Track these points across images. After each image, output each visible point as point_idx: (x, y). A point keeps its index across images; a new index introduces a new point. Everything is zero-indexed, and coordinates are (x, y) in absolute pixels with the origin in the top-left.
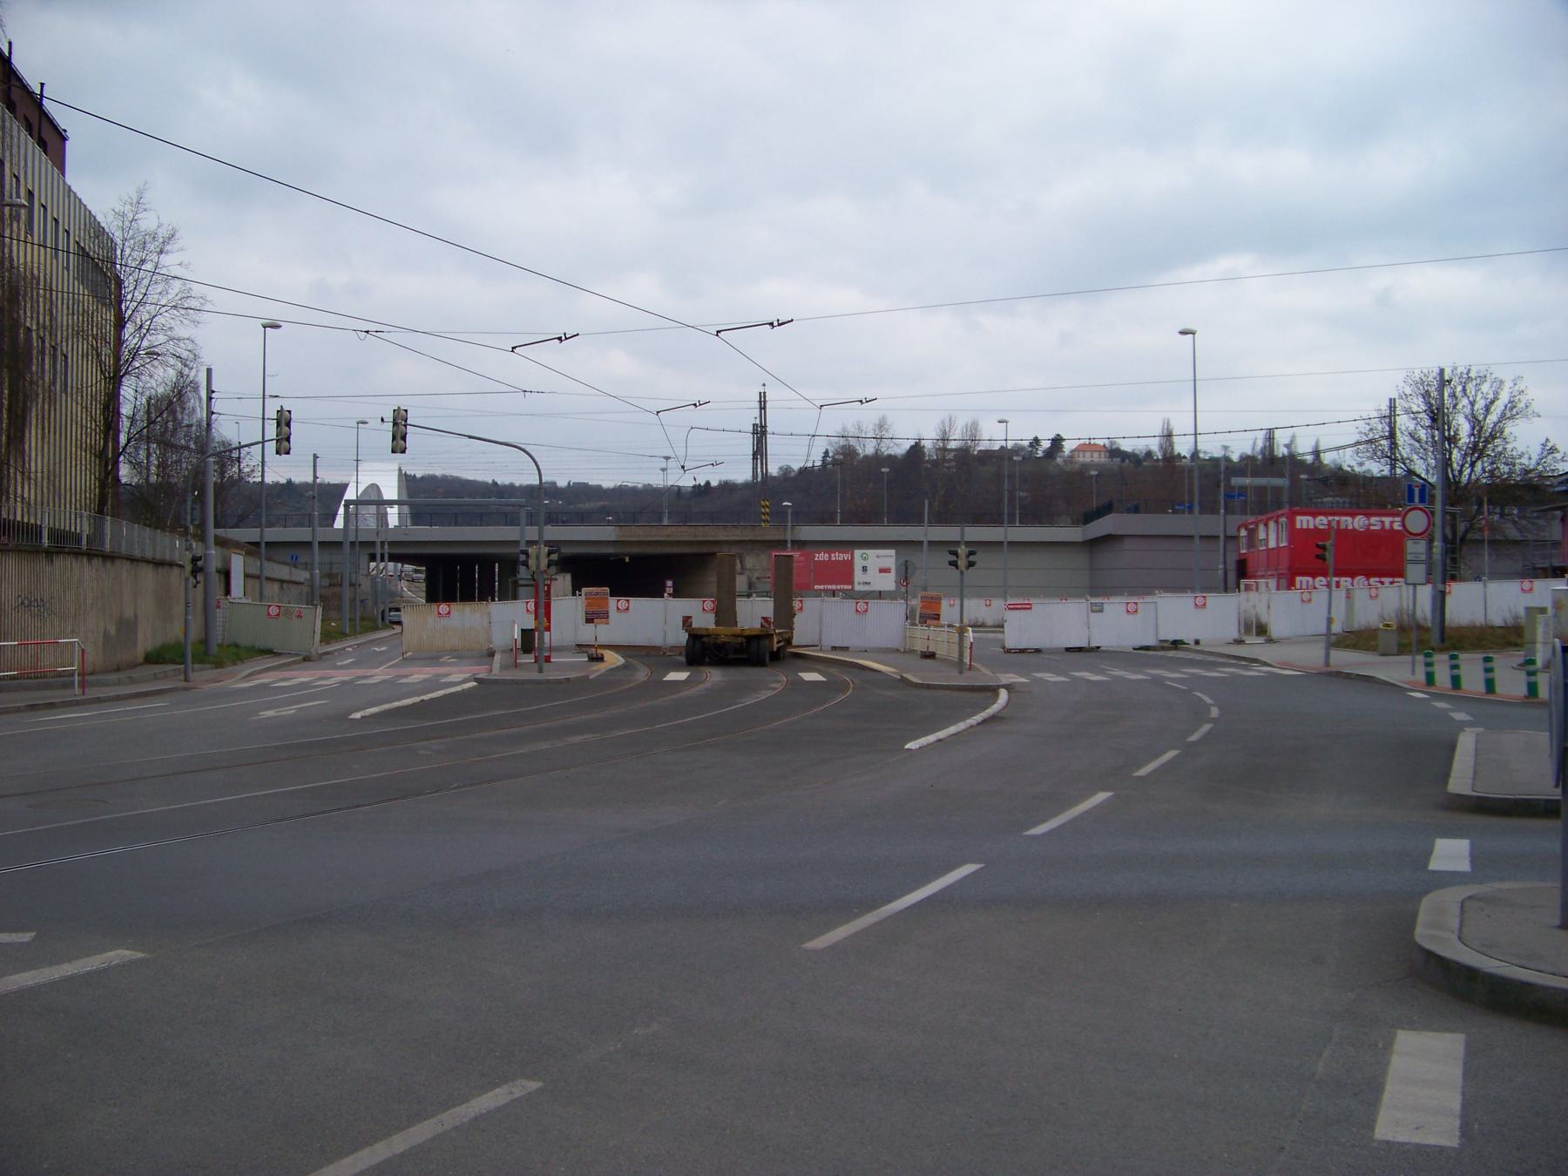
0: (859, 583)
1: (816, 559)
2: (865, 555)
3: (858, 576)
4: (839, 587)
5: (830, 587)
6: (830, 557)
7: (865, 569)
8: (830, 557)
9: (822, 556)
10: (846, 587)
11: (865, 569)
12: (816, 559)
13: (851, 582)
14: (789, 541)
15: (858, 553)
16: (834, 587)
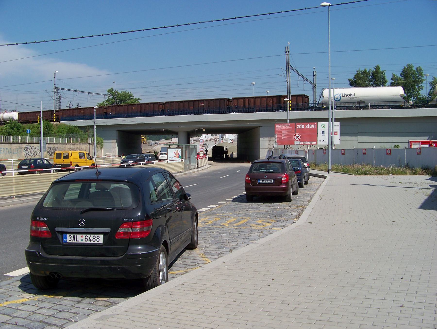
0: (320, 141)
1: (298, 128)
2: (323, 125)
3: (320, 137)
4: (309, 143)
5: (305, 143)
6: (305, 126)
7: (323, 133)
8: (305, 126)
9: (300, 126)
10: (313, 143)
11: (323, 133)
12: (298, 128)
13: (316, 140)
15: (320, 124)
16: (307, 143)
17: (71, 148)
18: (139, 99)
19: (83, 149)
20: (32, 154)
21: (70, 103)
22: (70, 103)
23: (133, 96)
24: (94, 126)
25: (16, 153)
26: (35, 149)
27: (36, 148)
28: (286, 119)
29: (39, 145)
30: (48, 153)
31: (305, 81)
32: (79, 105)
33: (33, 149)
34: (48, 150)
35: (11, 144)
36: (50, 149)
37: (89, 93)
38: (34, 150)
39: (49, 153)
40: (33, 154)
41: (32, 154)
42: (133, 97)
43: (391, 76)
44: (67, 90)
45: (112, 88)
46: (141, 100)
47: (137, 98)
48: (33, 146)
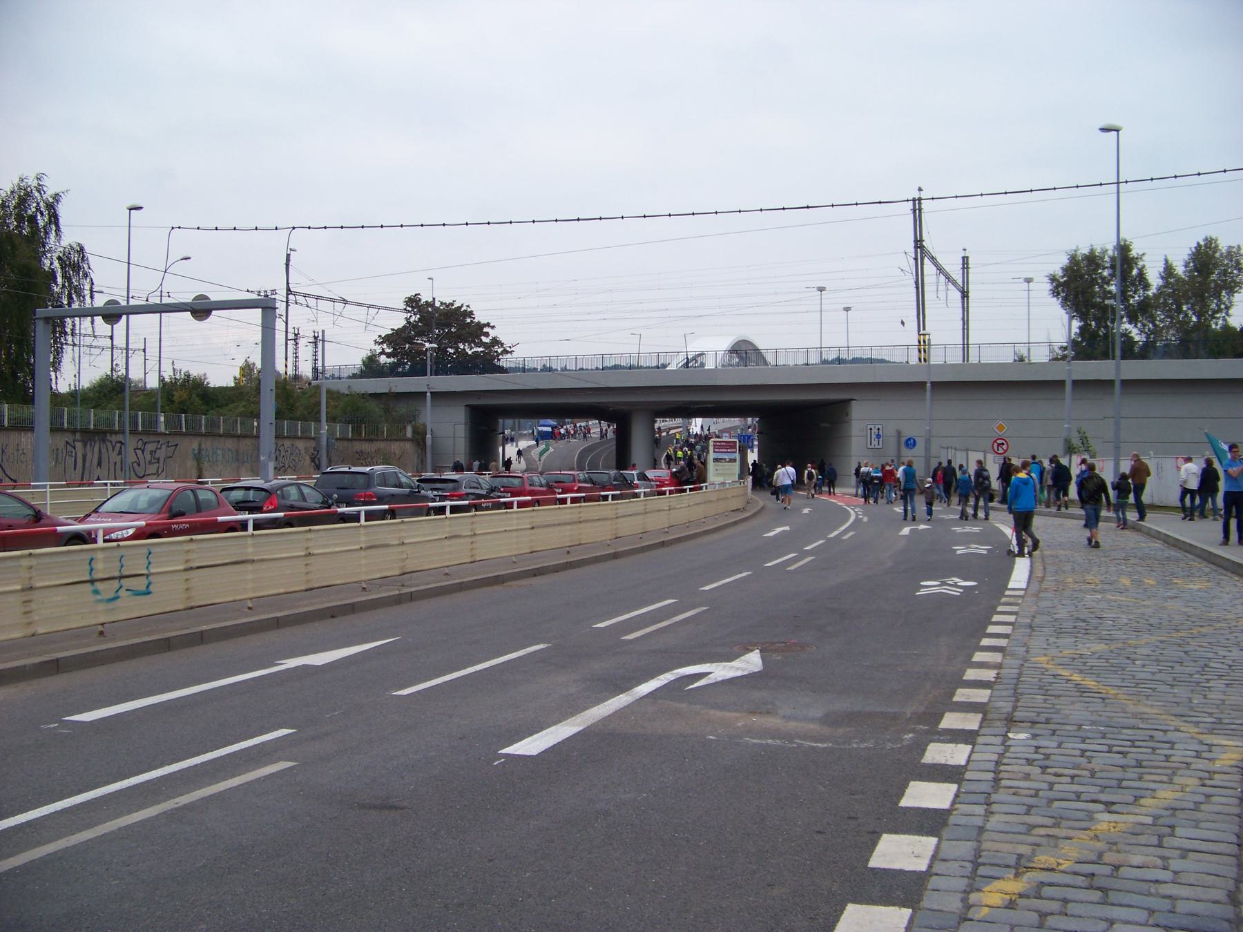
14: (929, 382)
17: (361, 451)
18: (488, 325)
19: (395, 454)
20: (280, 463)
21: (296, 330)
22: (296, 332)
23: (473, 316)
24: (426, 392)
25: (247, 462)
26: (287, 451)
27: (289, 449)
28: (925, 383)
29: (312, 444)
30: (313, 464)
31: (950, 283)
32: (298, 334)
33: (283, 453)
34: (313, 454)
35: (239, 437)
36: (316, 452)
37: (369, 306)
38: (284, 454)
39: (315, 463)
40: (282, 465)
41: (280, 463)
42: (474, 318)
43: (1160, 267)
44: (317, 298)
45: (416, 295)
46: (493, 327)
47: (483, 321)
48: (283, 445)
